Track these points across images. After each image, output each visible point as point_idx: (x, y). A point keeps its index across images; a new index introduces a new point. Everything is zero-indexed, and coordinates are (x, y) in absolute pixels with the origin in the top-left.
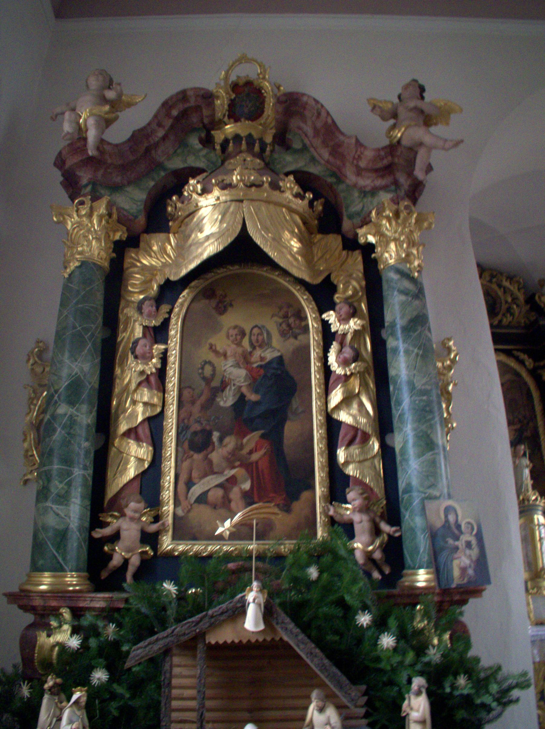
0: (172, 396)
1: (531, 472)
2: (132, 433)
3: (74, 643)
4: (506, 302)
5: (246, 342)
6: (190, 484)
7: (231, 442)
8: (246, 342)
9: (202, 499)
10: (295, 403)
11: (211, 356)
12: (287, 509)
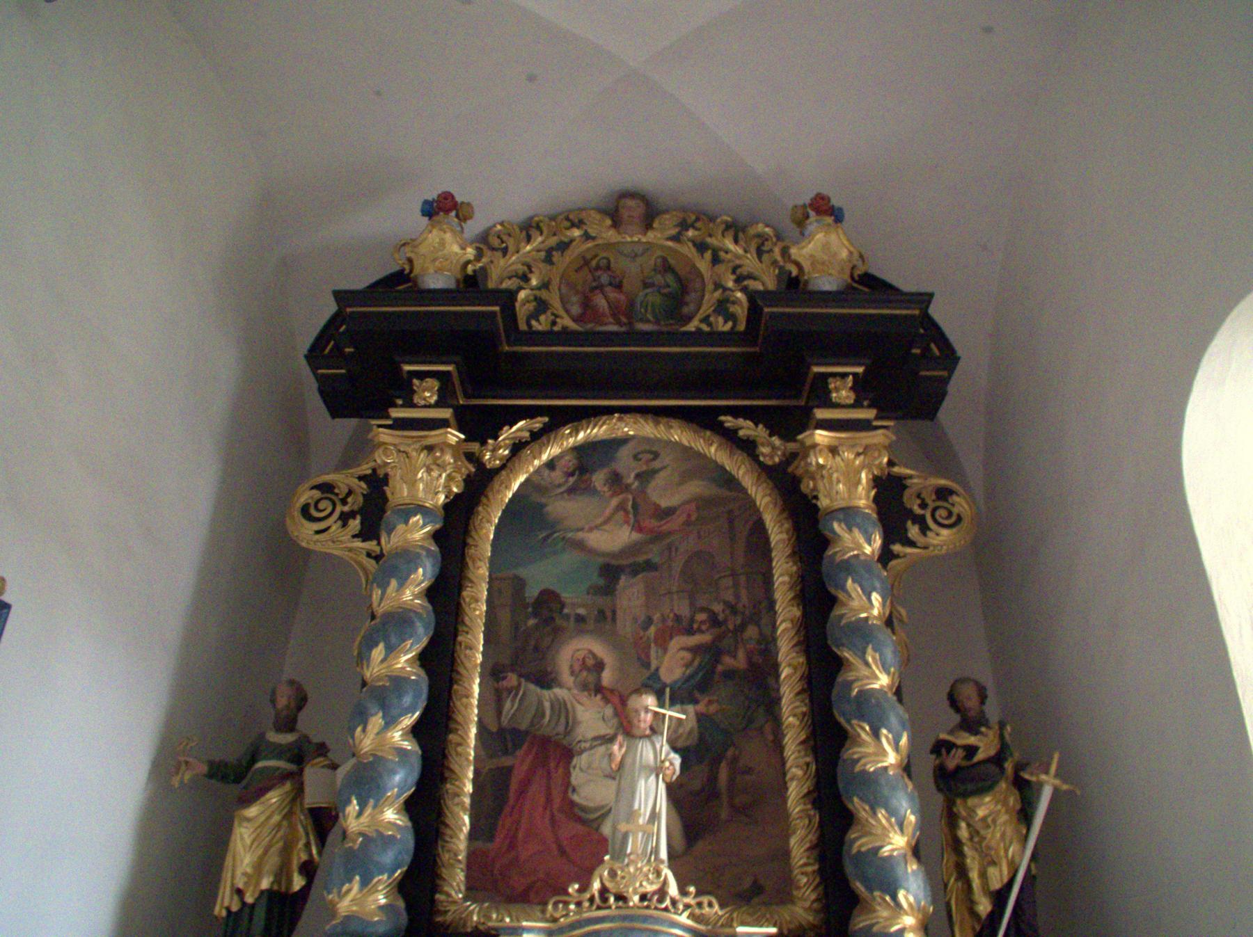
4: (718, 286)
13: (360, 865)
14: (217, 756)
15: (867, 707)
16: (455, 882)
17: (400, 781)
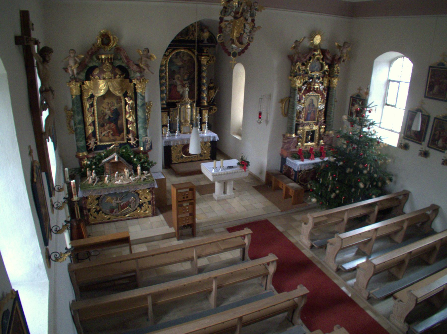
0: (96, 117)
1: (189, 92)
2: (90, 125)
3: (89, 163)
5: (109, 105)
6: (101, 133)
7: (108, 125)
8: (109, 105)
9: (104, 135)
10: (120, 117)
11: (103, 109)
12: (119, 136)
14: (53, 54)
15: (204, 84)
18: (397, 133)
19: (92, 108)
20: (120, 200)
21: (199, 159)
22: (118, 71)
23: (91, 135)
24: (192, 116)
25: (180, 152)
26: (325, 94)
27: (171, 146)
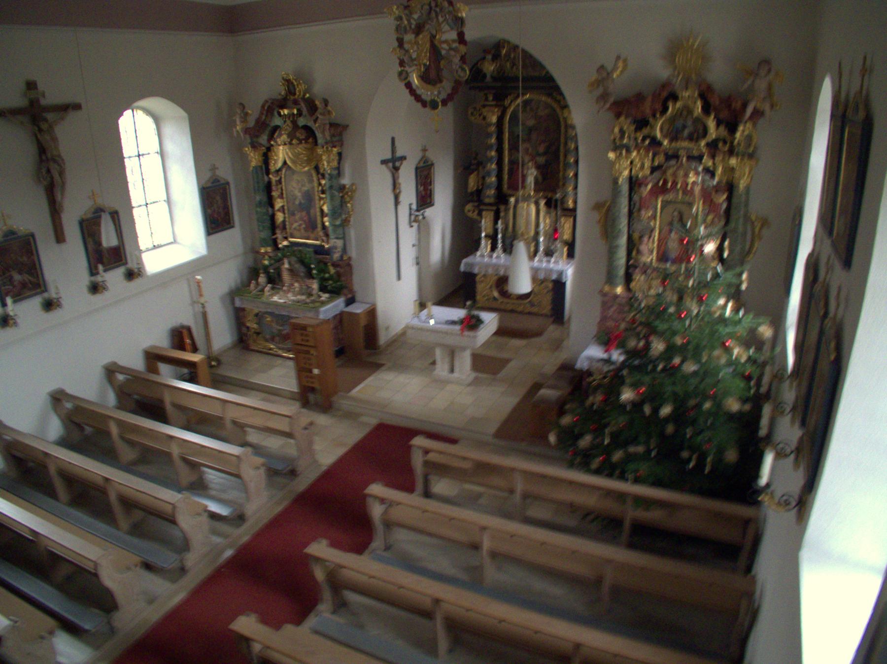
1: (536, 179)
2: (279, 210)
13: (489, 187)
16: (505, 186)
17: (494, 173)
18: (148, 250)
19: (279, 186)
20: (281, 326)
21: (527, 311)
22: (301, 135)
23: (281, 226)
24: (537, 225)
25: (491, 287)
26: (722, 198)
27: (474, 275)
